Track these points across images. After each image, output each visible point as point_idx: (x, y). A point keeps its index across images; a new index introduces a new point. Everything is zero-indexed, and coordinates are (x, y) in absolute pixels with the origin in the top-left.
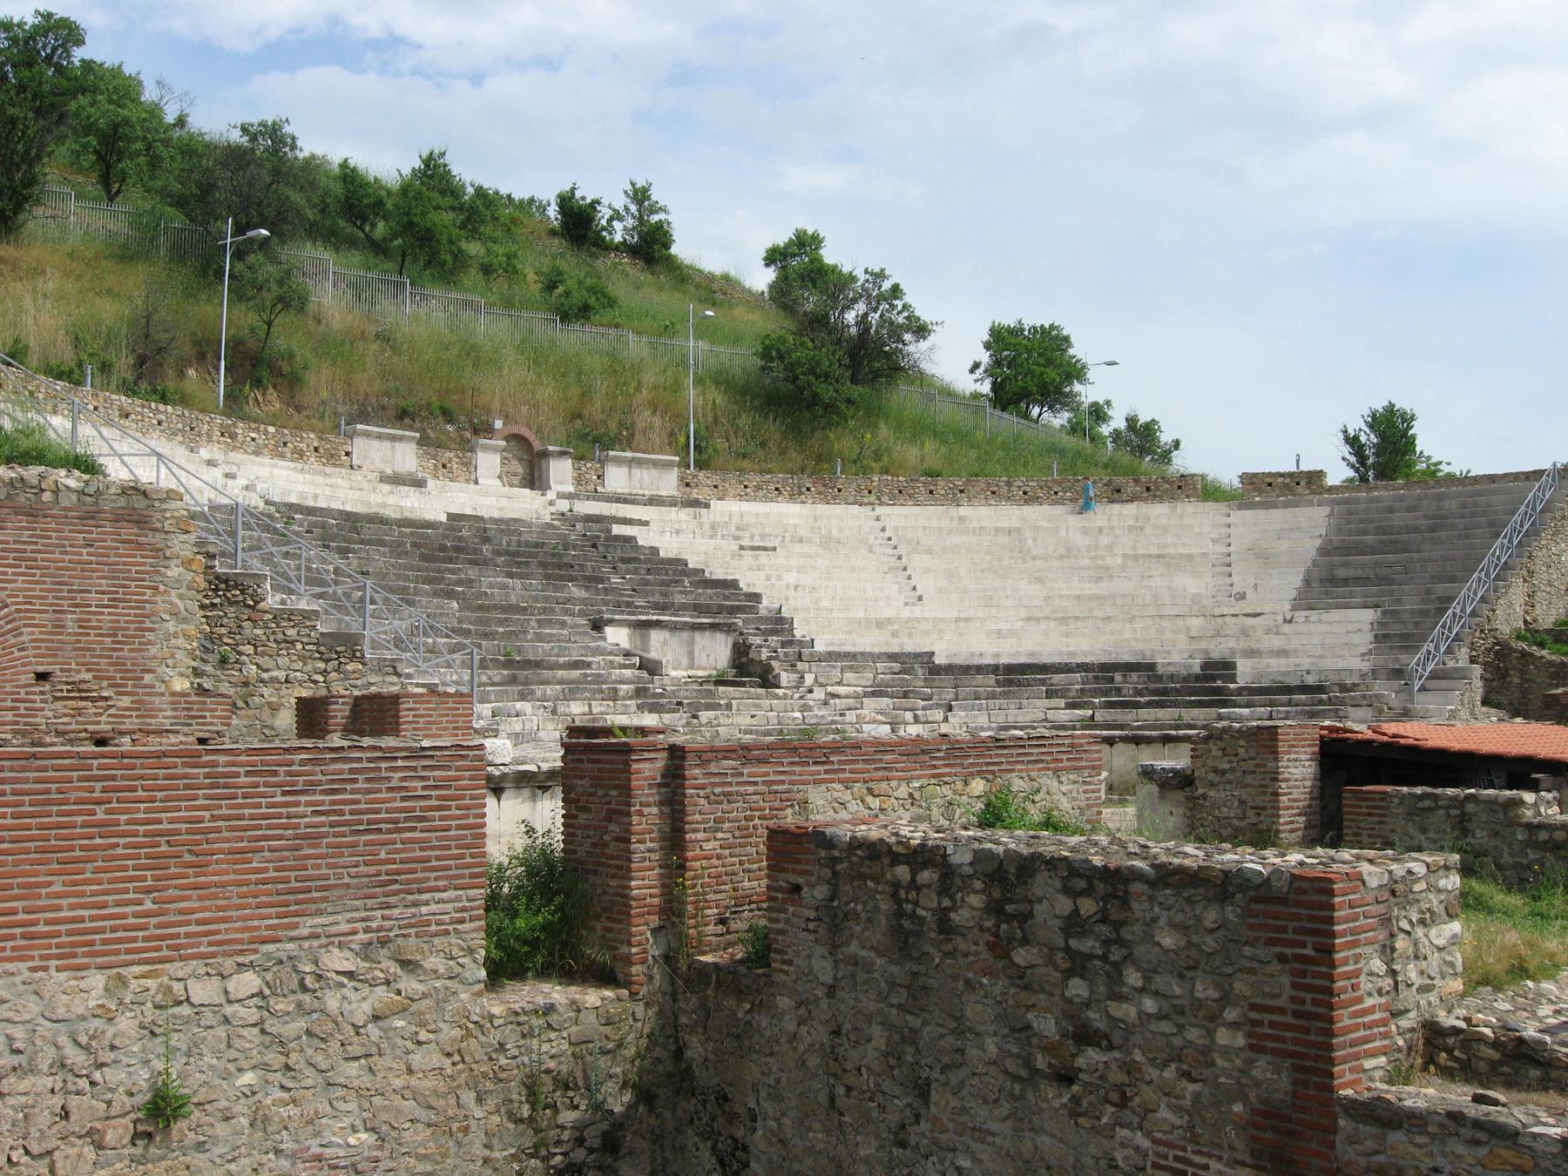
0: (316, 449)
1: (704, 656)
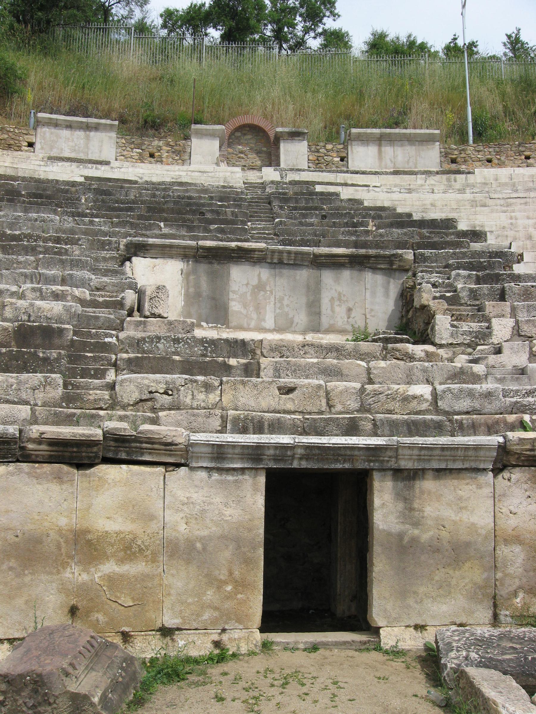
1: (340, 311)
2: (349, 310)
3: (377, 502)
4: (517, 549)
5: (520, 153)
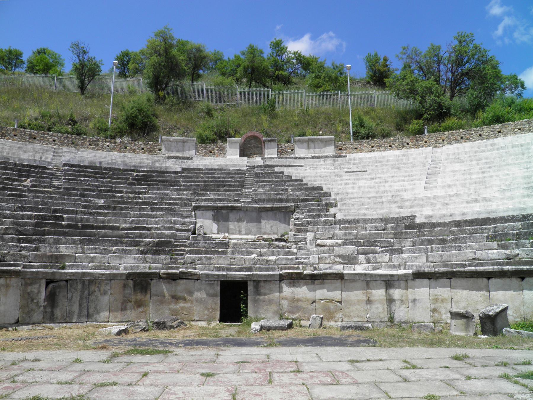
0: (143, 149)
2: (272, 227)
3: (249, 289)
4: (286, 301)
5: (370, 145)
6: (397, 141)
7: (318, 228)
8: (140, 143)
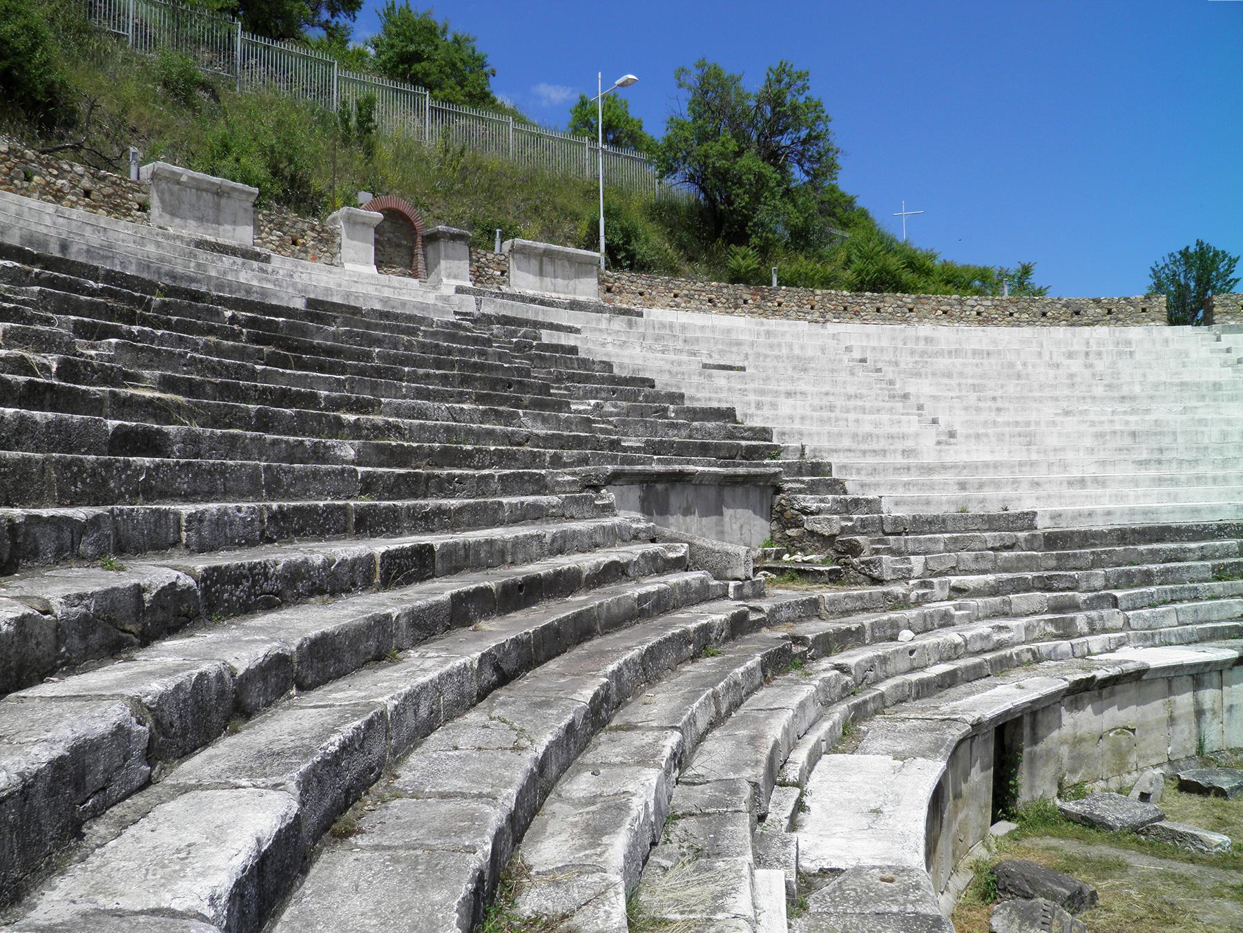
0: (87, 193)
2: (741, 527)
5: (670, 290)
6: (725, 291)
7: (906, 541)
8: (79, 169)
